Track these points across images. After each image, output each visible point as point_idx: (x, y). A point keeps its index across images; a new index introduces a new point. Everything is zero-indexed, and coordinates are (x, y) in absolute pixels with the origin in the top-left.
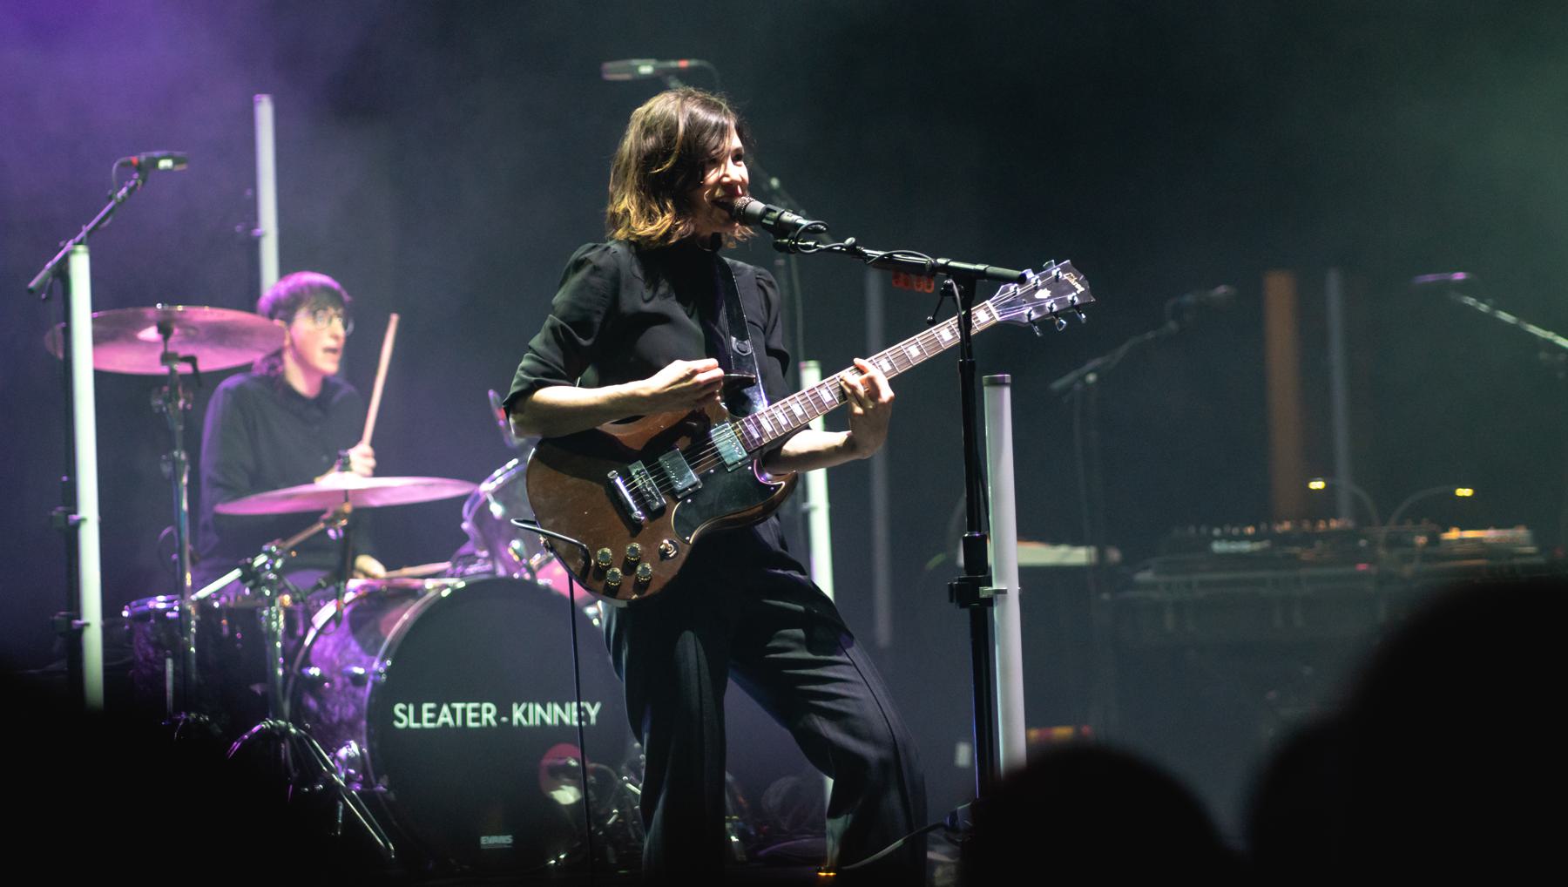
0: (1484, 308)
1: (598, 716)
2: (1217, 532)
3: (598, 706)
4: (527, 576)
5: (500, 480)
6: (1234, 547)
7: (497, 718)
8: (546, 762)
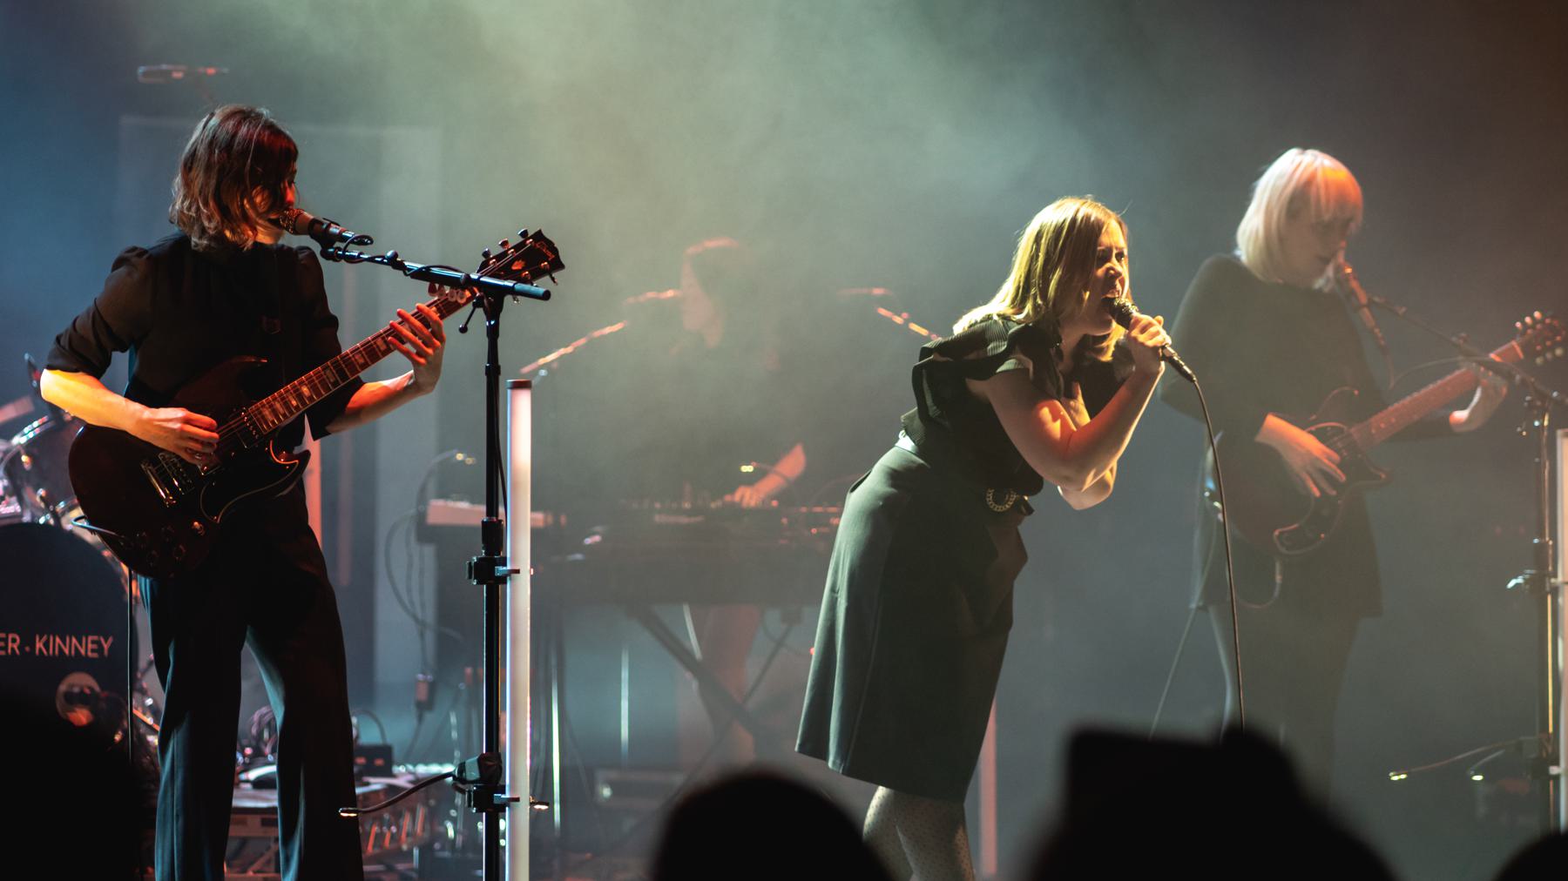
0: (898, 320)
1: (111, 649)
2: (658, 505)
3: (110, 640)
4: (52, 522)
5: (31, 435)
6: (672, 519)
7: (21, 648)
8: (63, 688)
